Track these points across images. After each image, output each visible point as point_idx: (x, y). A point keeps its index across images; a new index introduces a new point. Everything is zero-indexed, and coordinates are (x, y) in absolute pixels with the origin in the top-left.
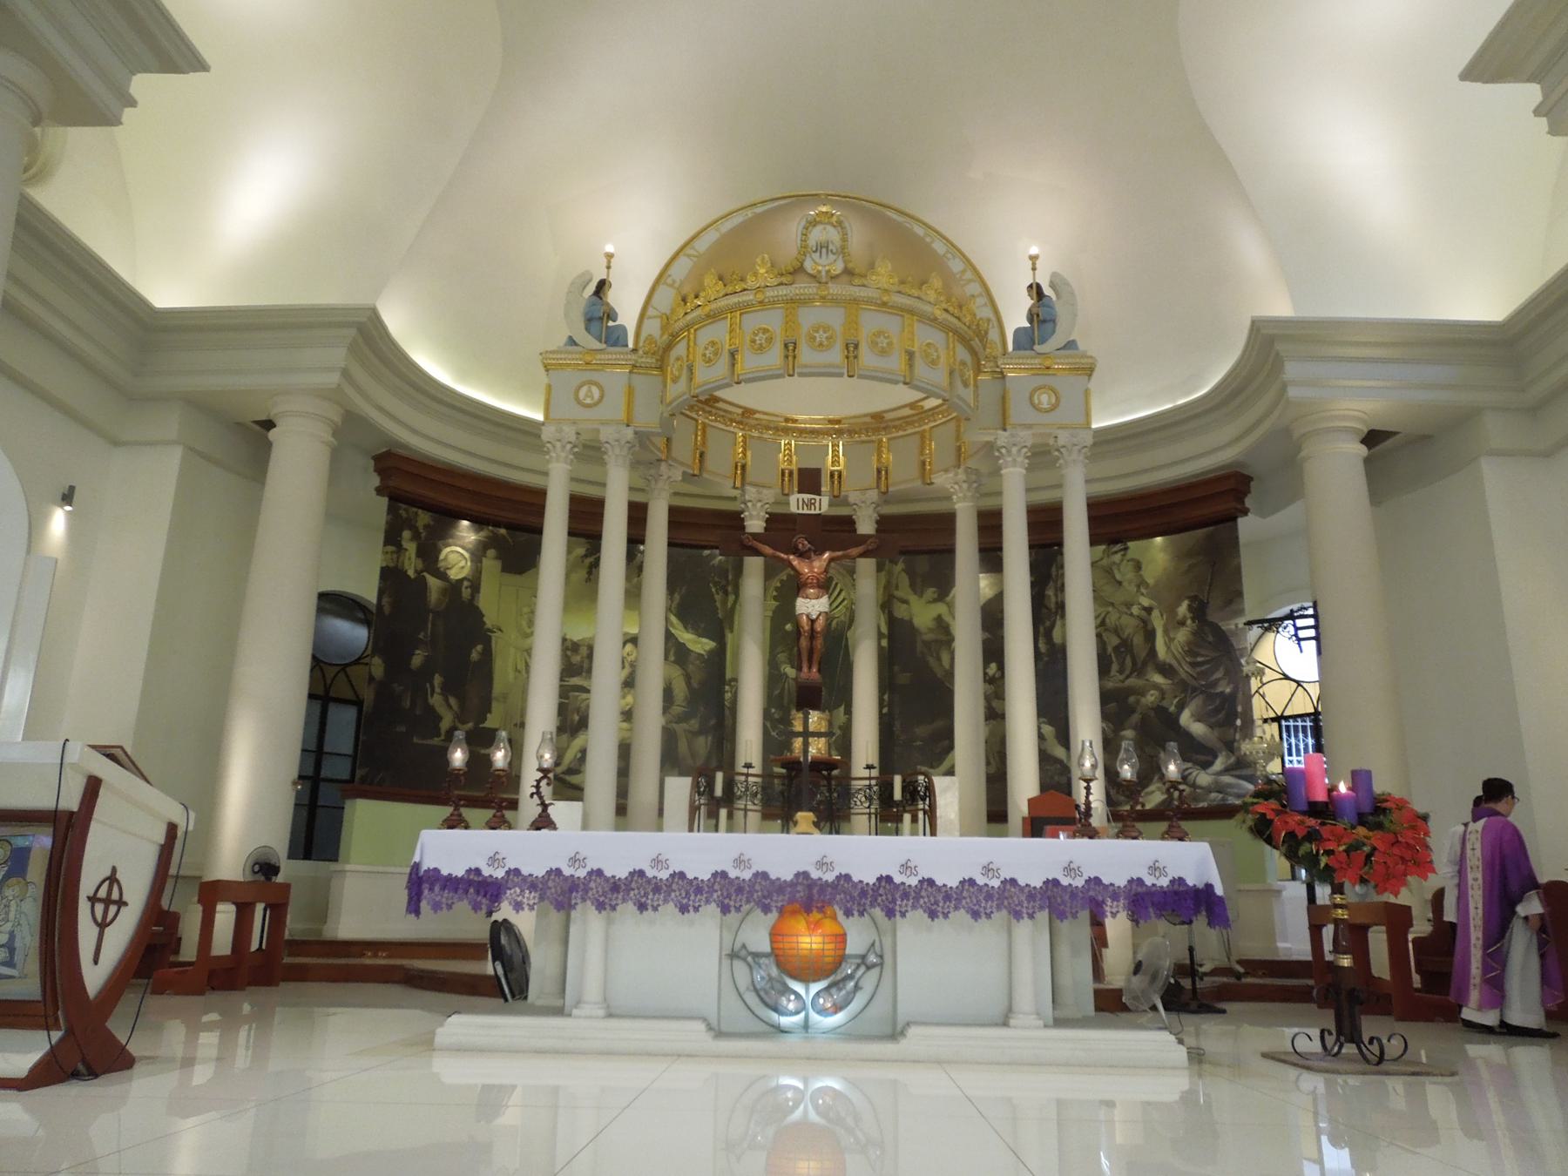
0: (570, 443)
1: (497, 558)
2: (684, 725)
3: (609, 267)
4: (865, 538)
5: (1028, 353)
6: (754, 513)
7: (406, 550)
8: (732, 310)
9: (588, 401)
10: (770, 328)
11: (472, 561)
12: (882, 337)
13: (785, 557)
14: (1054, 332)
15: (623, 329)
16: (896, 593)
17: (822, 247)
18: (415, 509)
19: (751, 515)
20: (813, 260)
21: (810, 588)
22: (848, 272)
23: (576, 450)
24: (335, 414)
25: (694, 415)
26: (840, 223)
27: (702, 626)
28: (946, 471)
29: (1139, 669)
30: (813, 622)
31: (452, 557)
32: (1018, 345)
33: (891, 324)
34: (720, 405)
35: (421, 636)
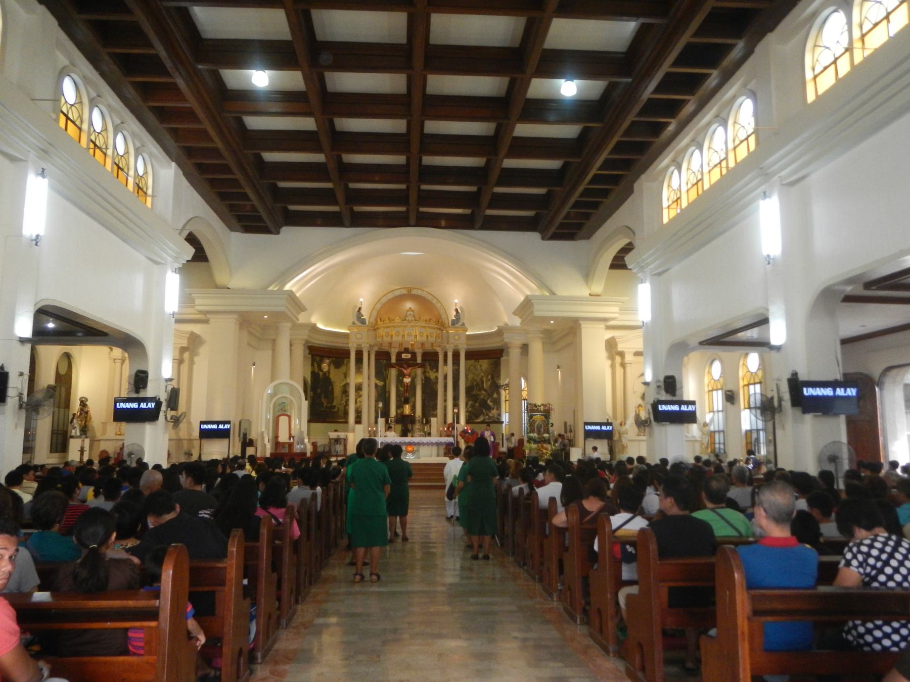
1: (334, 365)
4: (419, 364)
5: (453, 326)
14: (459, 322)
15: (365, 319)
16: (427, 370)
17: (410, 315)
22: (415, 320)
24: (303, 342)
29: (480, 390)
30: (407, 384)
32: (452, 325)
33: (423, 330)
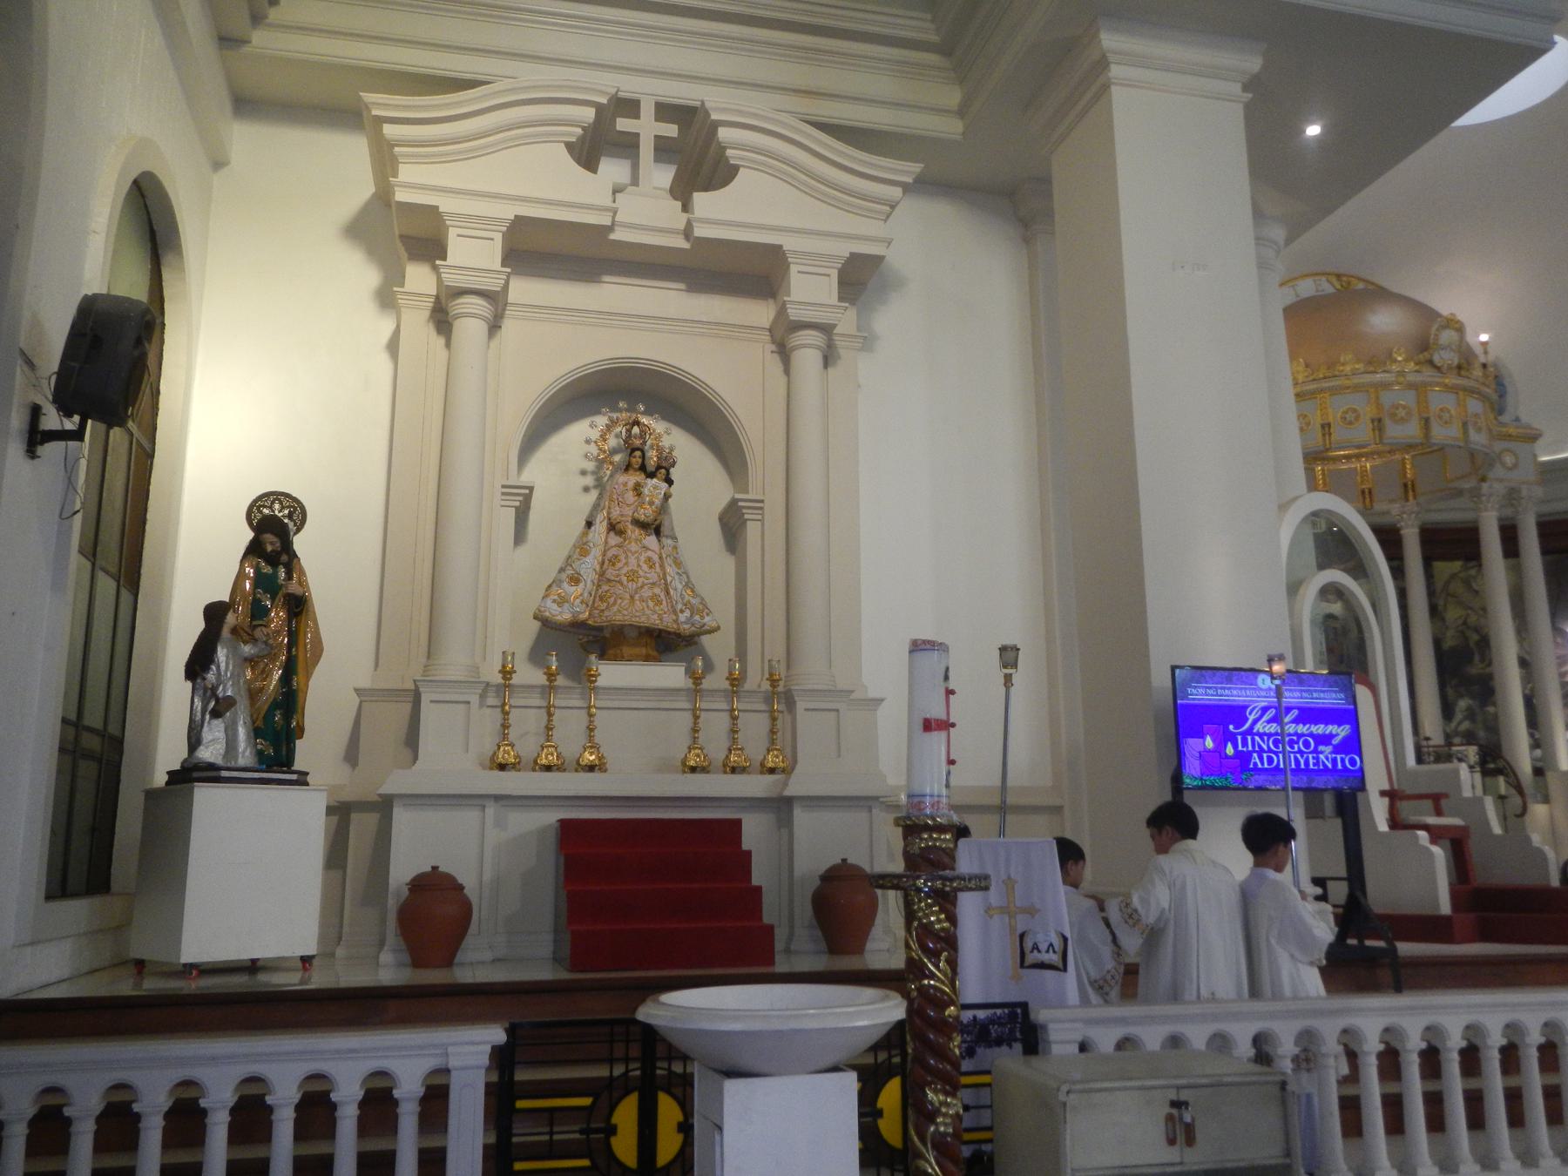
22: (1459, 367)
28: (1392, 501)
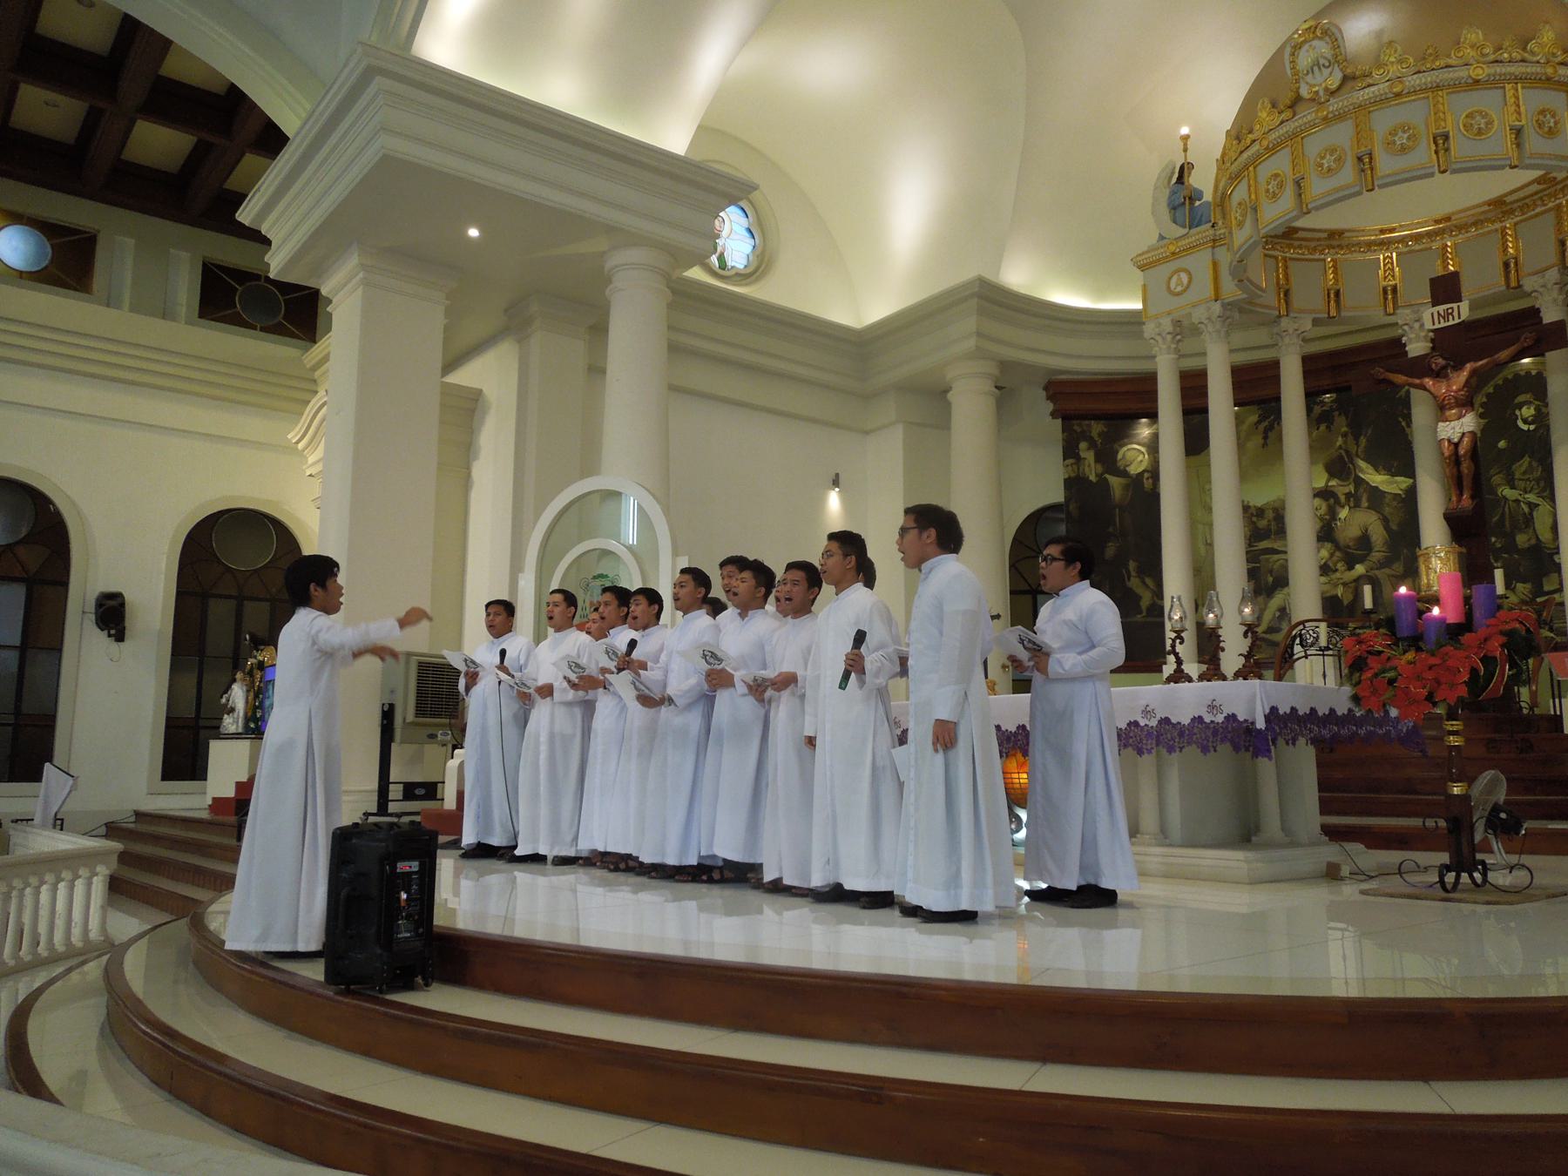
0: (1169, 333)
2: (1387, 571)
3: (1185, 150)
6: (1412, 336)
7: (1085, 459)
8: (1246, 167)
9: (1179, 289)
10: (1280, 172)
11: (1149, 454)
12: (1400, 134)
13: (1417, 381)
18: (1087, 422)
19: (1410, 340)
20: (1307, 83)
21: (1451, 408)
22: (1346, 79)
23: (1179, 337)
25: (1317, 256)
26: (1326, 32)
27: (1395, 465)
30: (1456, 445)
31: (1130, 455)
33: (1414, 113)
34: (1347, 234)
35: (1111, 530)
